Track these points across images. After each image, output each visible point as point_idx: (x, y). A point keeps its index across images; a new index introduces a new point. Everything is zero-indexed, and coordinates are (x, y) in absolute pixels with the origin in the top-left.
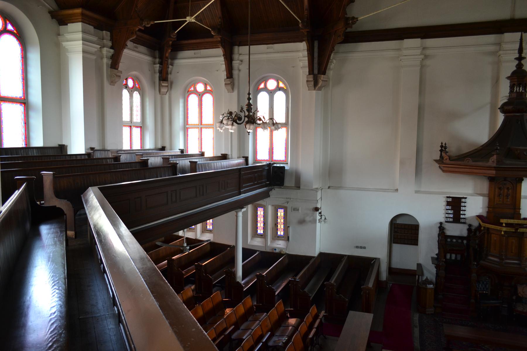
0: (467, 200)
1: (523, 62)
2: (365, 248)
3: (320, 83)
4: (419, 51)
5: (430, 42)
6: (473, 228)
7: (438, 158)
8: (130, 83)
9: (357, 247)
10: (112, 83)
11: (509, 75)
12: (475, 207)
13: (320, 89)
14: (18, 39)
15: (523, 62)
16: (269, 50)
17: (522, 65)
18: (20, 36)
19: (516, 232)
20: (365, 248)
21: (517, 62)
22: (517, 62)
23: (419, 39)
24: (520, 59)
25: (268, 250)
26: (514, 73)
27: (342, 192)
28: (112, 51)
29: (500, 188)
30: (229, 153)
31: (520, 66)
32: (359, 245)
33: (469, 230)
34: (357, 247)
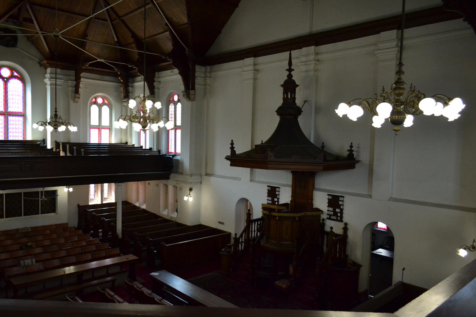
0: (281, 190)
1: (292, 73)
2: (223, 223)
3: (191, 96)
4: (252, 68)
5: (261, 59)
7: (229, 154)
8: (100, 101)
9: (219, 222)
10: (74, 101)
11: (283, 84)
12: (285, 197)
13: (193, 100)
14: (20, 80)
15: (292, 73)
16: (172, 73)
17: (292, 76)
18: (22, 79)
20: (223, 223)
21: (288, 73)
22: (288, 73)
23: (252, 58)
24: (290, 70)
25: (169, 219)
26: (285, 82)
27: (212, 178)
28: (75, 82)
30: (152, 147)
31: (290, 76)
32: (221, 221)
34: (219, 222)
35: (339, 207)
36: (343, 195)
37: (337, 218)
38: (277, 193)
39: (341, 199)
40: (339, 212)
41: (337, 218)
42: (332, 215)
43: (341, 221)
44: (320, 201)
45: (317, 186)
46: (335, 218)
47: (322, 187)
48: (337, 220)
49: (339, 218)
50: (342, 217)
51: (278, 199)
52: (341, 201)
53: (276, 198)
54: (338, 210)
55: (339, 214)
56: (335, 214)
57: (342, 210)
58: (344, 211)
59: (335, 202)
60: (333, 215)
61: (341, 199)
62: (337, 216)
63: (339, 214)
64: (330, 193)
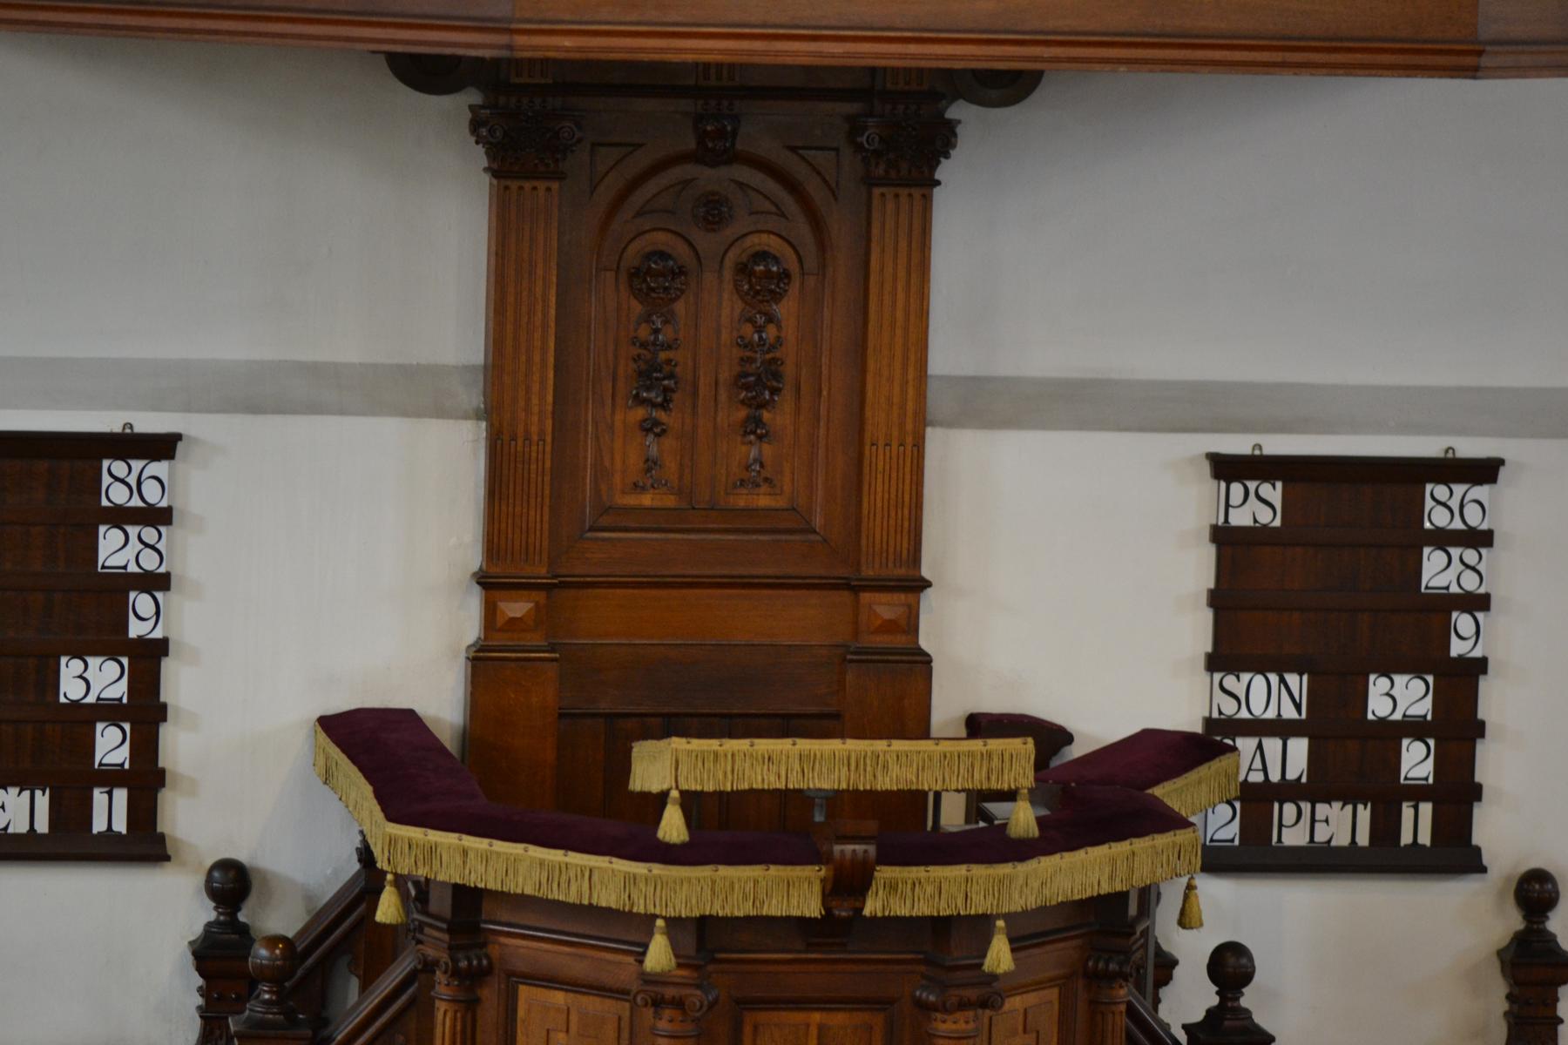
6: (278, 918)
19: (838, 927)
29: (656, 281)
33: (221, 957)
35: (1421, 632)
36: (1470, 448)
37: (1386, 827)
38: (115, 549)
39: (1441, 507)
40: (1414, 728)
41: (1386, 827)
42: (1288, 791)
43: (1454, 854)
44: (1066, 594)
45: (948, 355)
46: (1341, 824)
47: (1041, 356)
48: (1383, 857)
49: (1416, 825)
50: (1457, 793)
51: (147, 659)
52: (1443, 539)
53: (112, 642)
54: (1398, 696)
55: (1416, 762)
56: (1351, 757)
57: (1459, 683)
58: (1493, 700)
59: (1337, 568)
60: (1318, 788)
61: (1441, 507)
62: (1387, 797)
63: (1416, 762)
64: (1237, 445)
